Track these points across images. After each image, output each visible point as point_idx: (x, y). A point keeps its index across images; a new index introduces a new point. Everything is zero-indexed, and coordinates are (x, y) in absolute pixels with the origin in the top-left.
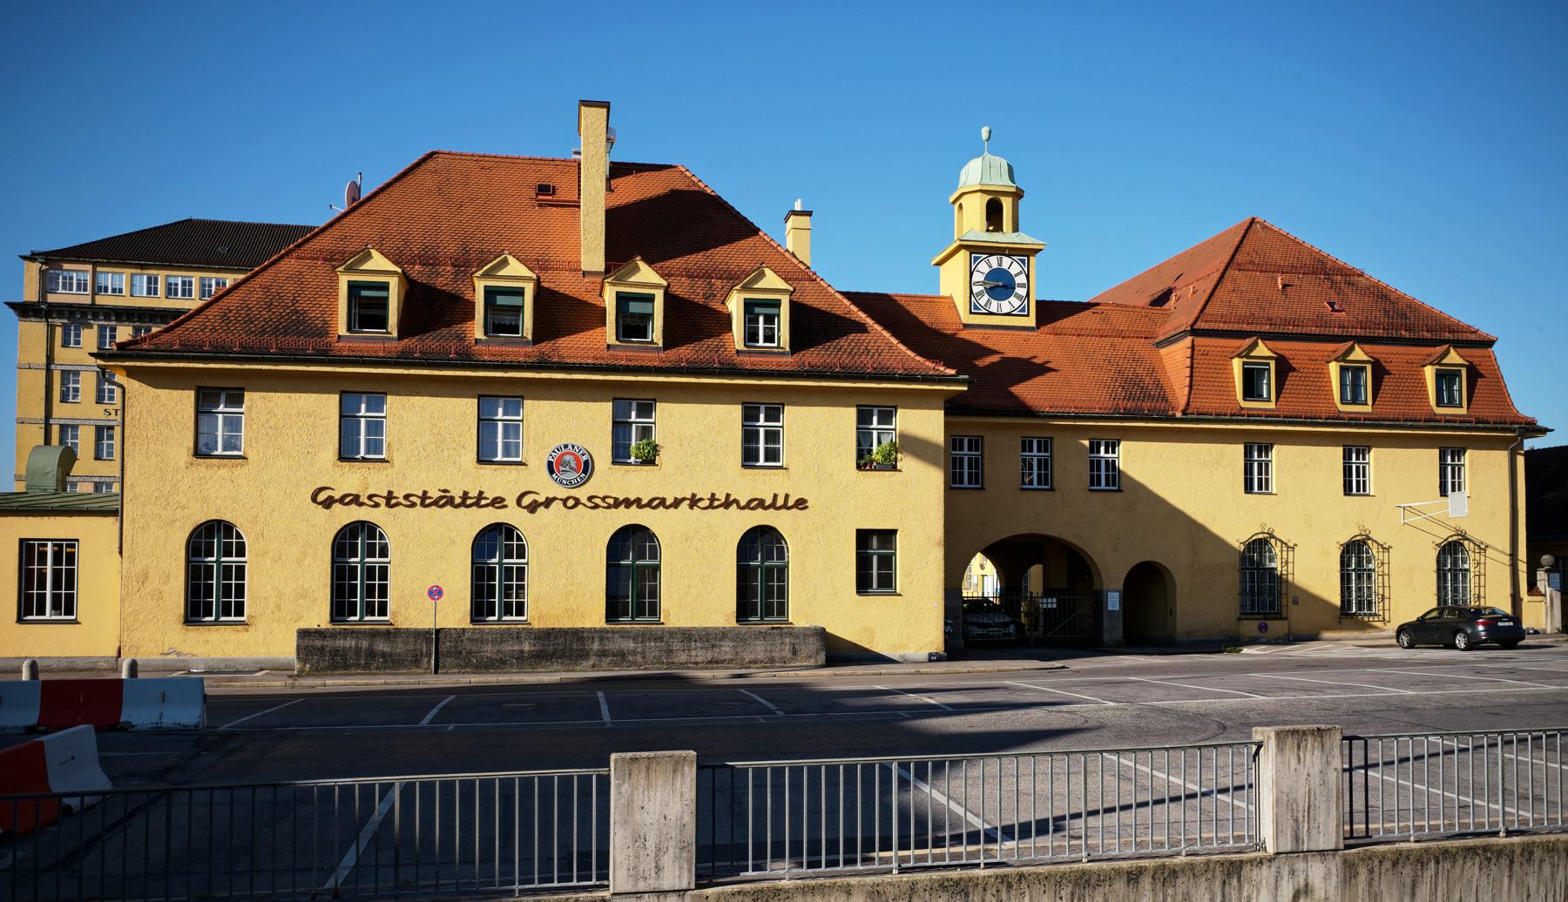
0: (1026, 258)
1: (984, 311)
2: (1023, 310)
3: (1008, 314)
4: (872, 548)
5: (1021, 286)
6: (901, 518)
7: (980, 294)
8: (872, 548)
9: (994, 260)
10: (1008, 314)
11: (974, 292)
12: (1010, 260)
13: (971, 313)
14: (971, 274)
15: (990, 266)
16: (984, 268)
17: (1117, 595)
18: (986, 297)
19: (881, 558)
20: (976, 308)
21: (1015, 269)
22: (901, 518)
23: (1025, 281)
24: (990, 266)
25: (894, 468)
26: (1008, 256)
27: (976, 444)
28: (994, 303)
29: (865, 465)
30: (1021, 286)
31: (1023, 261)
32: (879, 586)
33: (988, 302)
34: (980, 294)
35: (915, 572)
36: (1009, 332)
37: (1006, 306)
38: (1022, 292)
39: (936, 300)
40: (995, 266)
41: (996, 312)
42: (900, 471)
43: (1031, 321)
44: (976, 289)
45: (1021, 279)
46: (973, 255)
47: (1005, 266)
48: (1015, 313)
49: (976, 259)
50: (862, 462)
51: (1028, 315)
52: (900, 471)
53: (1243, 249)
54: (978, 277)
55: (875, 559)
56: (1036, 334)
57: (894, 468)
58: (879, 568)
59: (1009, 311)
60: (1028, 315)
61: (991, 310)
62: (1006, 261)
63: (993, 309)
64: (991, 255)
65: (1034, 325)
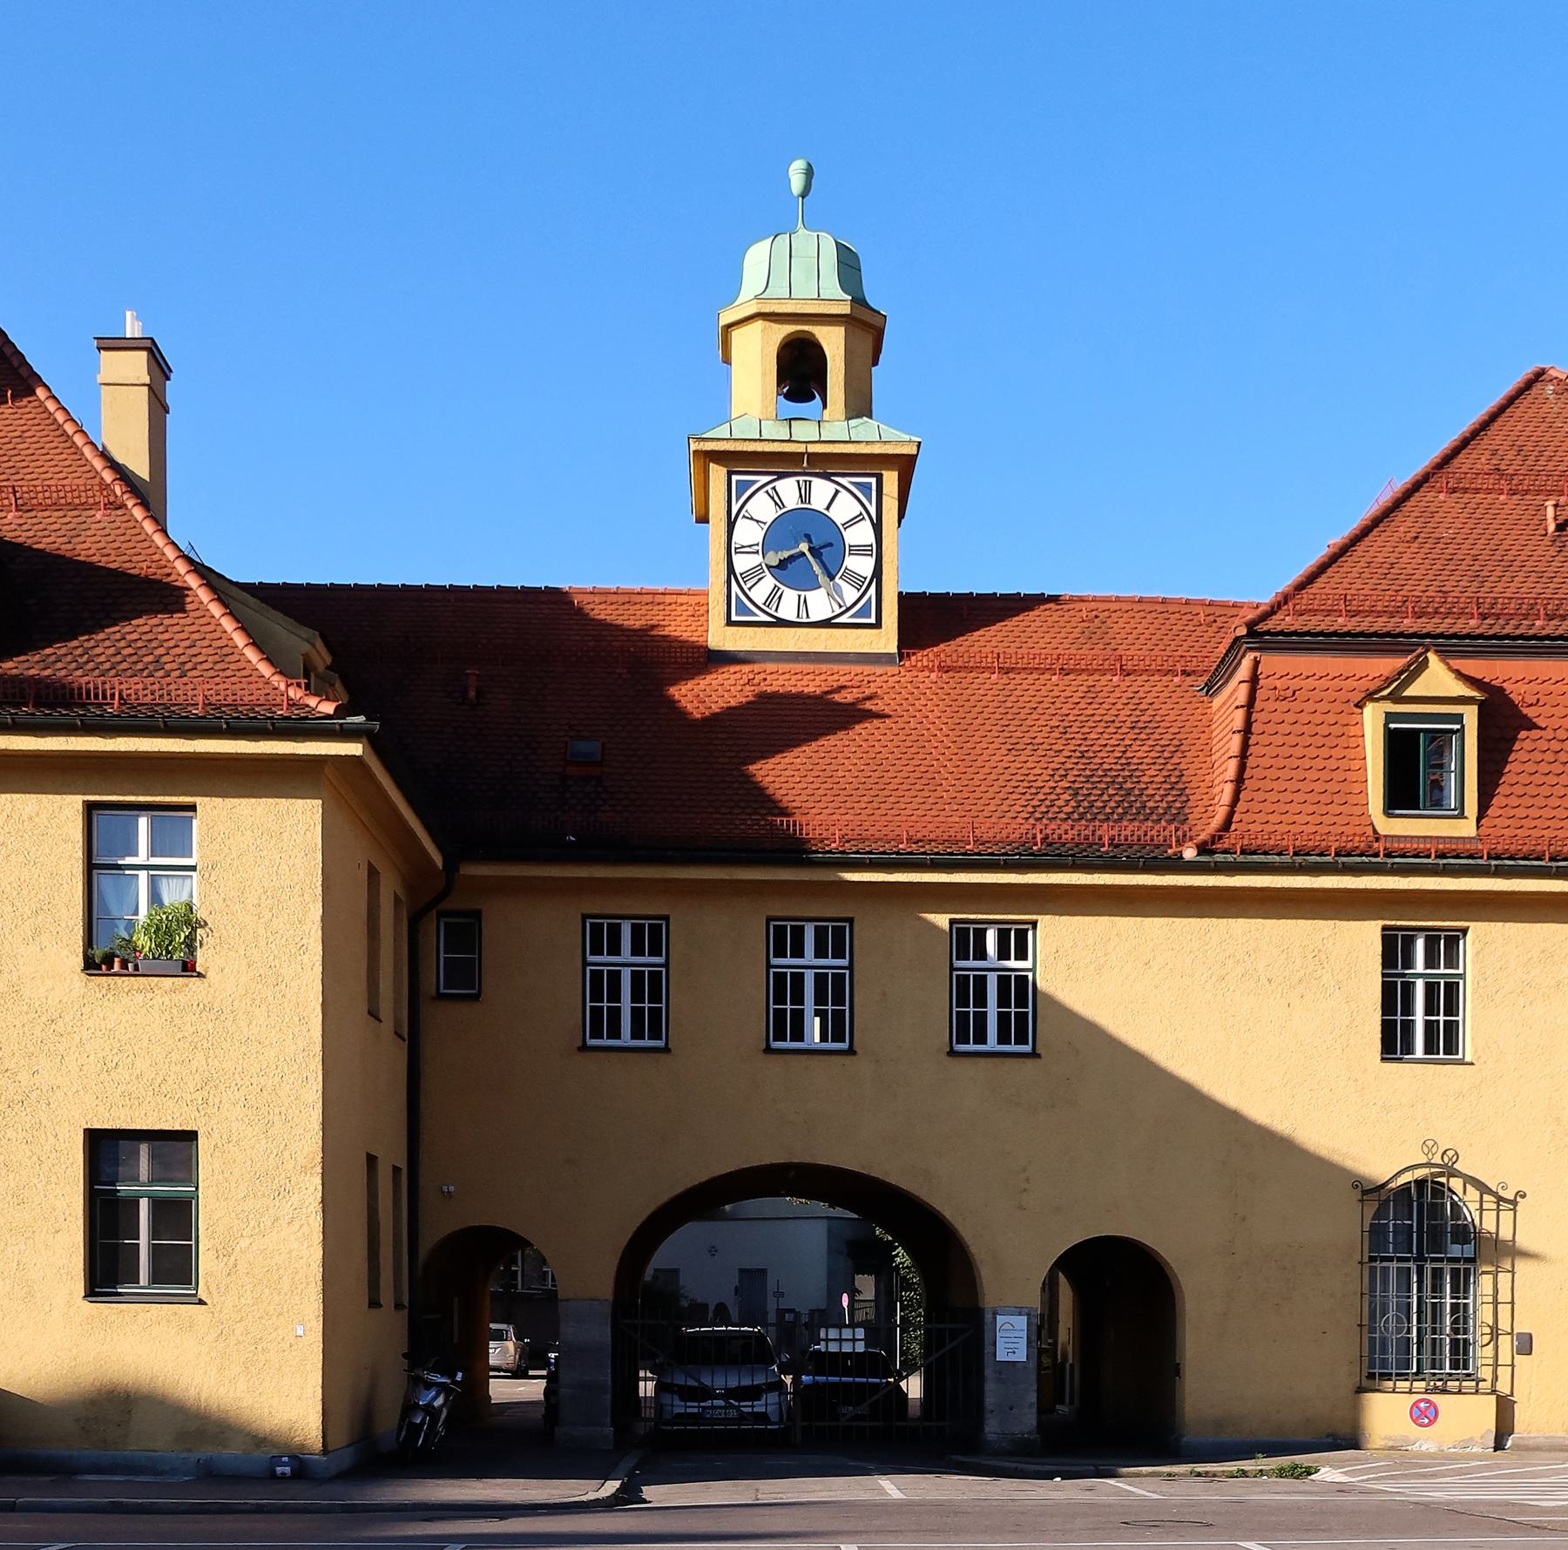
0: (873, 481)
1: (764, 618)
2: (864, 612)
3: (826, 624)
4: (135, 1179)
5: (859, 550)
6: (205, 1101)
7: (755, 574)
8: (135, 1179)
9: (788, 489)
10: (826, 624)
11: (739, 569)
12: (833, 487)
13: (730, 623)
14: (731, 526)
15: (779, 504)
16: (762, 508)
17: (1021, 1322)
18: (769, 582)
19: (158, 1204)
20: (742, 609)
21: (844, 509)
22: (205, 1101)
23: (869, 538)
24: (779, 504)
25: (188, 968)
26: (827, 476)
27: (651, 938)
28: (790, 597)
29: (108, 960)
30: (859, 550)
31: (865, 488)
32: (156, 1279)
33: (775, 596)
34: (755, 574)
35: (244, 1243)
36: (824, 667)
37: (820, 604)
38: (863, 566)
39: (668, 599)
40: (791, 500)
41: (793, 618)
42: (200, 975)
43: (886, 640)
44: (742, 563)
45: (861, 534)
46: (735, 478)
47: (818, 502)
48: (843, 619)
49: (743, 486)
50: (98, 953)
51: (878, 625)
52: (200, 975)
53: (1485, 442)
54: (748, 533)
55: (144, 1204)
56: (895, 670)
57: (188, 968)
58: (155, 1233)
59: (829, 615)
60: (878, 625)
61: (781, 614)
62: (821, 490)
63: (787, 611)
64: (781, 476)
65: (892, 648)
